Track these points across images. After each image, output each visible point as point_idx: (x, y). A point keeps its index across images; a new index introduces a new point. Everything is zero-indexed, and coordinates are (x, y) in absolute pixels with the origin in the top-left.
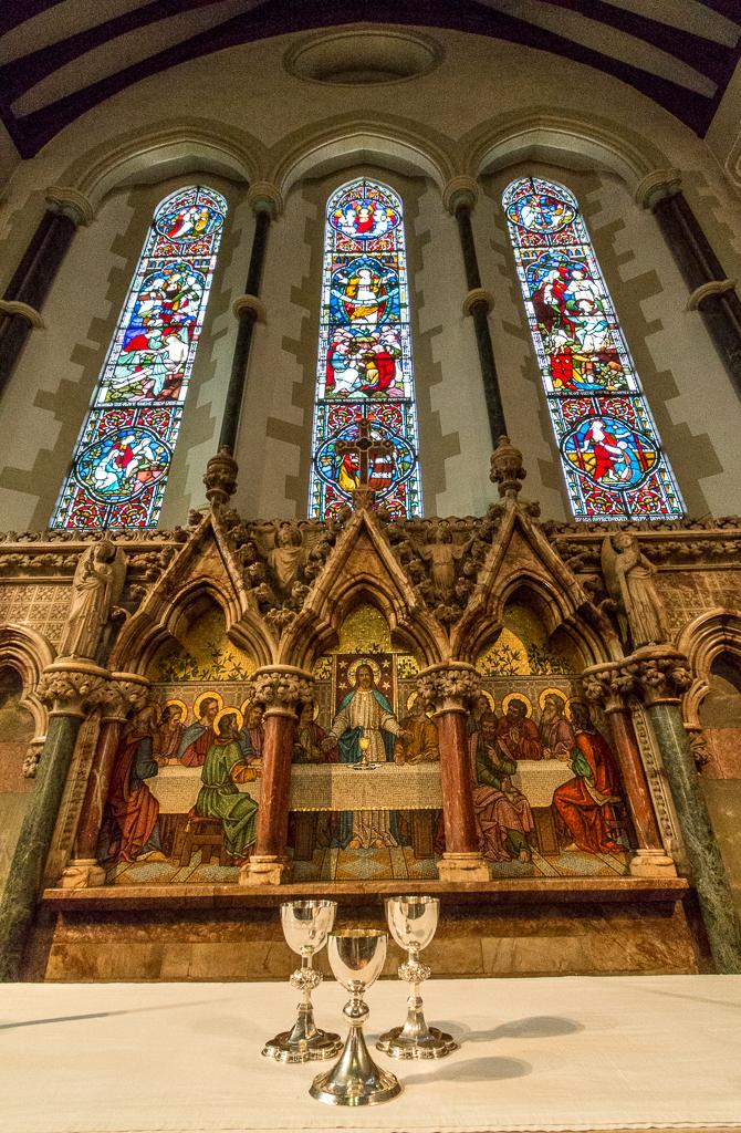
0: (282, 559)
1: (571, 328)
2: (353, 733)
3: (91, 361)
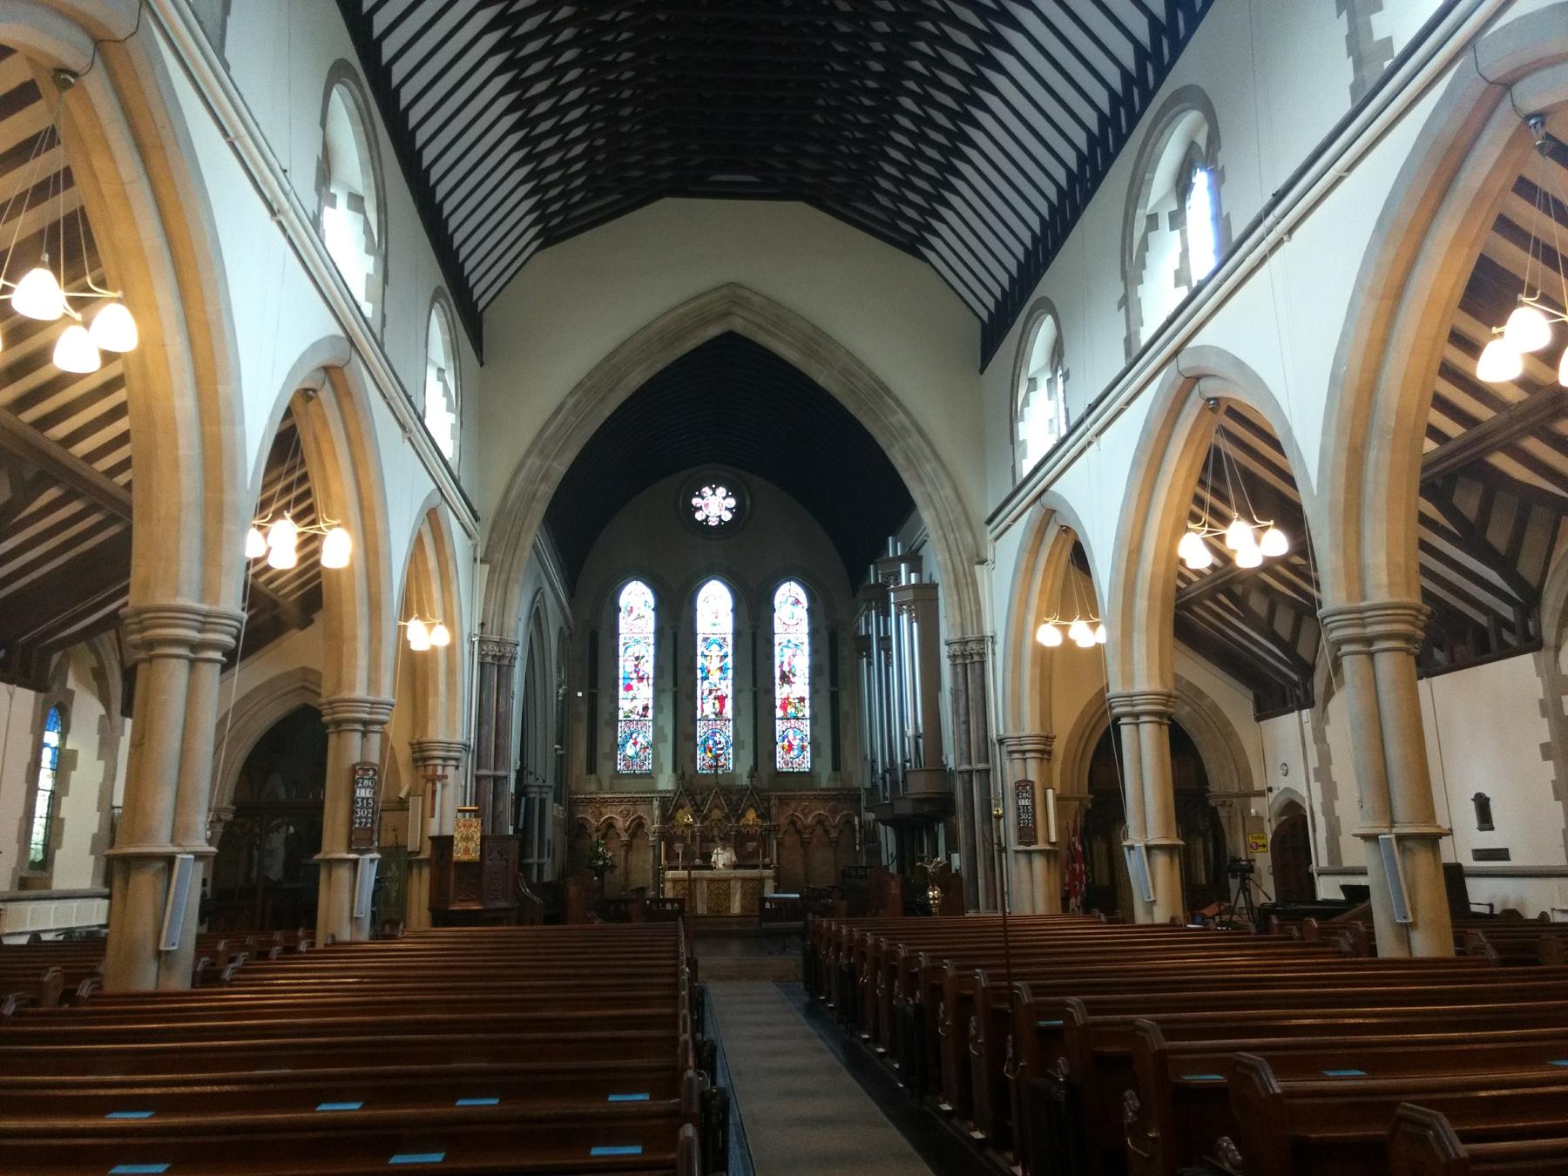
0: (698, 798)
1: (789, 682)
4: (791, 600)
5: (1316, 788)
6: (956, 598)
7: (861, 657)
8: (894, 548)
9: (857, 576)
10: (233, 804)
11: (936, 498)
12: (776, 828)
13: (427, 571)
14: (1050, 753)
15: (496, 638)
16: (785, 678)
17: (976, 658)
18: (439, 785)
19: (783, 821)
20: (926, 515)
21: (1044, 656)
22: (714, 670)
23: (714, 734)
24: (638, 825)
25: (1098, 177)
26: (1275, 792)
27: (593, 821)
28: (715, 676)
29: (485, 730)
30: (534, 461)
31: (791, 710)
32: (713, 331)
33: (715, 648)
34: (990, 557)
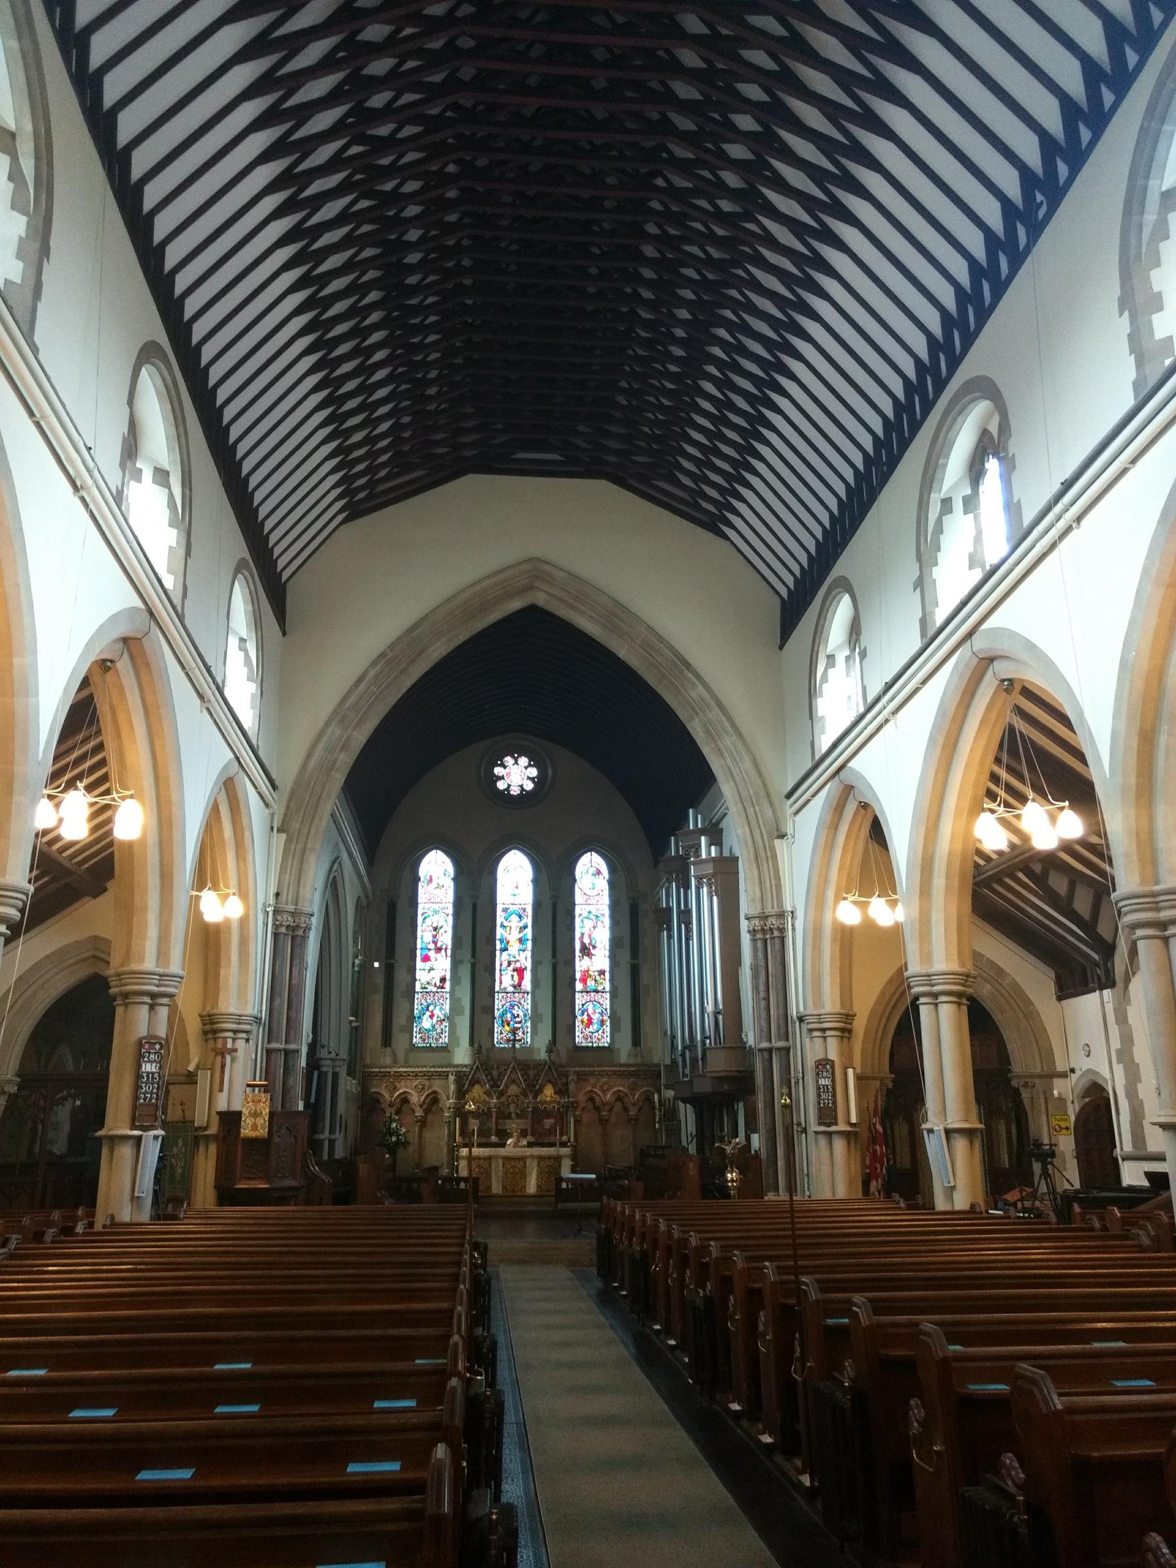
0: (495, 1073)
1: (589, 955)
2: (510, 1113)
3: (412, 970)
4: (593, 870)
5: (1119, 1070)
6: (755, 872)
7: (661, 930)
8: (694, 820)
9: (658, 847)
10: (18, 1075)
11: (735, 771)
12: (574, 1106)
13: (222, 840)
14: (850, 1031)
15: (291, 908)
16: (586, 951)
17: (776, 933)
18: (228, 1059)
19: (582, 1098)
20: (726, 788)
21: (845, 935)
22: (512, 943)
23: (512, 1007)
24: (434, 1100)
25: (894, 462)
26: (1078, 1073)
27: (387, 1095)
28: (514, 947)
29: (277, 1002)
30: (334, 731)
31: (591, 984)
32: (516, 605)
33: (514, 918)
34: (790, 831)
